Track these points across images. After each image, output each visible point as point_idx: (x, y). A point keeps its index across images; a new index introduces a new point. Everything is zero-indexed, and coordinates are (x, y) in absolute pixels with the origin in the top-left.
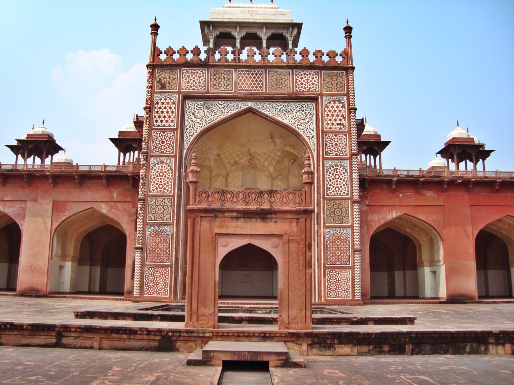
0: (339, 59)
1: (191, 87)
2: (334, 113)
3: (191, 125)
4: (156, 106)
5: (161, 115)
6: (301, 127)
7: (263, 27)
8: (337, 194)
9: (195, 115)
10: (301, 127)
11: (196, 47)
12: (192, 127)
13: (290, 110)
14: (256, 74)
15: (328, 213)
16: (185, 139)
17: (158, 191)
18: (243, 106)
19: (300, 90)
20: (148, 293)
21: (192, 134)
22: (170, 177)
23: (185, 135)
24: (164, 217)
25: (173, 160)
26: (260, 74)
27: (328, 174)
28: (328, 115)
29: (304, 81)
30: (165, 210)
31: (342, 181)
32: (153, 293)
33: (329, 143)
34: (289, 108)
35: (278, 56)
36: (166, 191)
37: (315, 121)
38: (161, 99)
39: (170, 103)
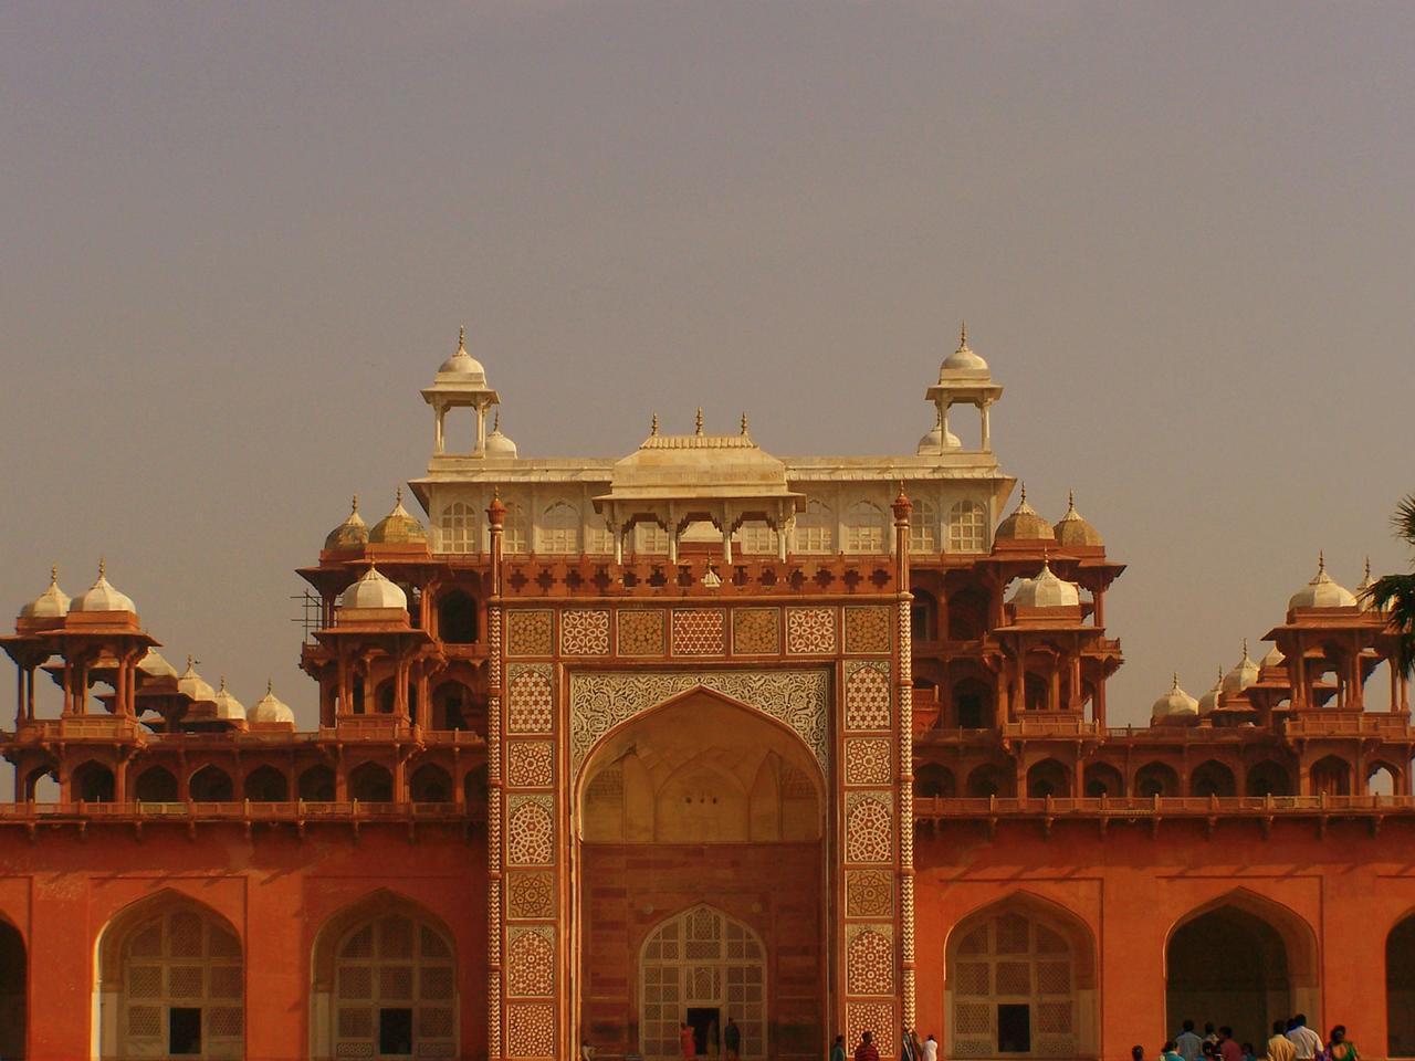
1: (581, 648)
5: (523, 708)
6: (799, 724)
10: (799, 724)
16: (572, 754)
18: (687, 684)
19: (797, 649)
20: (515, 1052)
21: (586, 743)
23: (572, 745)
25: (550, 797)
27: (852, 819)
28: (853, 700)
29: (805, 631)
31: (879, 832)
36: (540, 859)
38: (521, 676)
39: (541, 684)
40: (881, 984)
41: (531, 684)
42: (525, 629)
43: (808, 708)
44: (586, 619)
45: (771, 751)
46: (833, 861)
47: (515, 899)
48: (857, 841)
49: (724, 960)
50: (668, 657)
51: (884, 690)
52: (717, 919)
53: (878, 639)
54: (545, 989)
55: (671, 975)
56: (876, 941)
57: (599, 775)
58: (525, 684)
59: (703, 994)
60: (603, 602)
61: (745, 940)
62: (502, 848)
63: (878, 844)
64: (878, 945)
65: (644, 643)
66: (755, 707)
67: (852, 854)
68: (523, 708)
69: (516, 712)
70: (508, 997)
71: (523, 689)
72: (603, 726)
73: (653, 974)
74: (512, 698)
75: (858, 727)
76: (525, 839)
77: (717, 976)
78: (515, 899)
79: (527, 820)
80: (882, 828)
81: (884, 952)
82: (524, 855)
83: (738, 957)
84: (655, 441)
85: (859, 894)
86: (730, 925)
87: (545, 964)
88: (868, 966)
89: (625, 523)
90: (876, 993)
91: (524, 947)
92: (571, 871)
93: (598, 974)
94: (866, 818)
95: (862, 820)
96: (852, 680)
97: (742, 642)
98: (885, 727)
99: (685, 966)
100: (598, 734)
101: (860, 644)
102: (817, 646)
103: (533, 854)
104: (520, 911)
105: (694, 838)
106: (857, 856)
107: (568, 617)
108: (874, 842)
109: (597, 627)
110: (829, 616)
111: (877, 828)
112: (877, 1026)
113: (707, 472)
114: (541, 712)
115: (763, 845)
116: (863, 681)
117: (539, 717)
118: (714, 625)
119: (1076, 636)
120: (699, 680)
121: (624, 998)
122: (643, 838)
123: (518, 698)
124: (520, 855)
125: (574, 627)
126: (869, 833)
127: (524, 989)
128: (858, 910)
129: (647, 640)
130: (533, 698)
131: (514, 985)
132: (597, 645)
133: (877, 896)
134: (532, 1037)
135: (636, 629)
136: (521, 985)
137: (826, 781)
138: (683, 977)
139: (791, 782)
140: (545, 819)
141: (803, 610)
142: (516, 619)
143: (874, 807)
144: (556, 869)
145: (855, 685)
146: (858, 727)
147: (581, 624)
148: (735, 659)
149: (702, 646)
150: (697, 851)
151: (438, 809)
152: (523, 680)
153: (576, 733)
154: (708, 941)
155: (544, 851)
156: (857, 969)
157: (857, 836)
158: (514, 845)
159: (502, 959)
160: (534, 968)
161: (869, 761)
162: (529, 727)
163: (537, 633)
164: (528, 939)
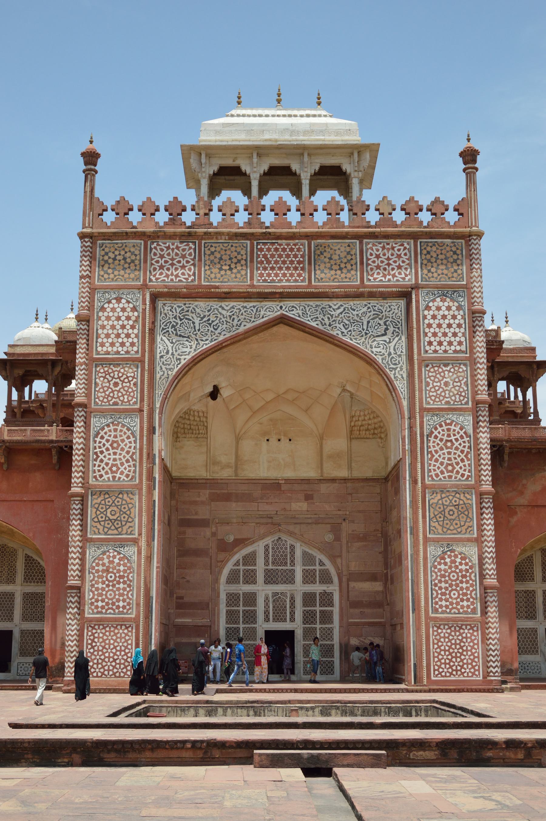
0: (451, 217)
2: (442, 321)
3: (170, 349)
4: (101, 314)
5: (110, 331)
6: (378, 350)
7: (302, 154)
8: (450, 477)
9: (175, 330)
10: (378, 350)
11: (176, 198)
12: (173, 354)
13: (355, 318)
14: (292, 250)
15: (432, 515)
16: (158, 376)
17: (109, 478)
19: (375, 279)
21: (171, 366)
22: (132, 450)
23: (158, 369)
24: (122, 526)
26: (299, 250)
27: (432, 439)
28: (430, 326)
29: (382, 262)
30: (125, 513)
31: (458, 452)
32: (103, 673)
33: (434, 381)
34: (355, 313)
35: (334, 213)
36: (123, 477)
37: (403, 338)
38: (109, 302)
39: (129, 310)
40: (465, 603)
41: (119, 310)
42: (114, 259)
43: (385, 334)
44: (173, 250)
45: (344, 390)
46: (414, 481)
47: (97, 516)
48: (437, 460)
49: (299, 587)
50: (253, 286)
51: (459, 317)
52: (292, 547)
53: (453, 271)
54: (124, 607)
55: (251, 599)
56: (458, 560)
57: (185, 413)
58: (113, 310)
59: (279, 617)
60: (190, 234)
61: (318, 567)
62: (86, 466)
63: (457, 464)
64: (461, 564)
65: (229, 272)
66: (334, 333)
67: (433, 473)
68: (110, 331)
69: (103, 336)
70: (86, 615)
71: (111, 314)
72: (188, 350)
73: (233, 599)
74: (100, 323)
75: (435, 351)
76: (108, 458)
77: (292, 599)
78: (97, 516)
79: (111, 439)
80: (461, 448)
81: (467, 571)
82: (107, 473)
84: (240, 112)
85: (440, 513)
86: (305, 554)
87: (124, 583)
88: (451, 585)
89: (212, 173)
90: (459, 613)
91: (104, 565)
92: (155, 489)
93: (182, 598)
94: (445, 438)
95: (441, 440)
96: (428, 308)
97: (322, 272)
98: (461, 351)
99: (263, 590)
100: (183, 357)
101: (435, 275)
102: (394, 276)
103: (116, 472)
104: (101, 528)
105: (273, 474)
106: (437, 475)
107: (155, 248)
108: (454, 461)
109: (184, 257)
110: (405, 248)
111: (457, 449)
112: (461, 647)
113: (287, 129)
114: (128, 336)
115: (333, 480)
116: (439, 309)
117: (125, 340)
118: (296, 256)
119: (535, 367)
120: (281, 307)
121: (205, 621)
122: (226, 474)
123: (106, 323)
124: (103, 472)
125: (162, 257)
126: (449, 453)
127: (103, 607)
128: (440, 528)
129: (231, 269)
130: (121, 323)
131: (92, 604)
132: (183, 274)
133: (459, 515)
134: (109, 657)
135: (221, 259)
136: (100, 604)
137: (405, 403)
139: (360, 423)
140: (128, 438)
141: (380, 243)
142: (107, 250)
143: (453, 427)
144: (139, 487)
145: (431, 313)
146: (435, 351)
147: (169, 254)
148: (316, 287)
149: (284, 275)
150: (273, 486)
151: (29, 433)
152: (111, 306)
153: (162, 357)
155: (126, 469)
156: (440, 588)
157: (436, 456)
158: (97, 463)
159: (82, 577)
160: (114, 586)
161: (446, 384)
162: (115, 349)
163: (126, 263)
164: (109, 557)
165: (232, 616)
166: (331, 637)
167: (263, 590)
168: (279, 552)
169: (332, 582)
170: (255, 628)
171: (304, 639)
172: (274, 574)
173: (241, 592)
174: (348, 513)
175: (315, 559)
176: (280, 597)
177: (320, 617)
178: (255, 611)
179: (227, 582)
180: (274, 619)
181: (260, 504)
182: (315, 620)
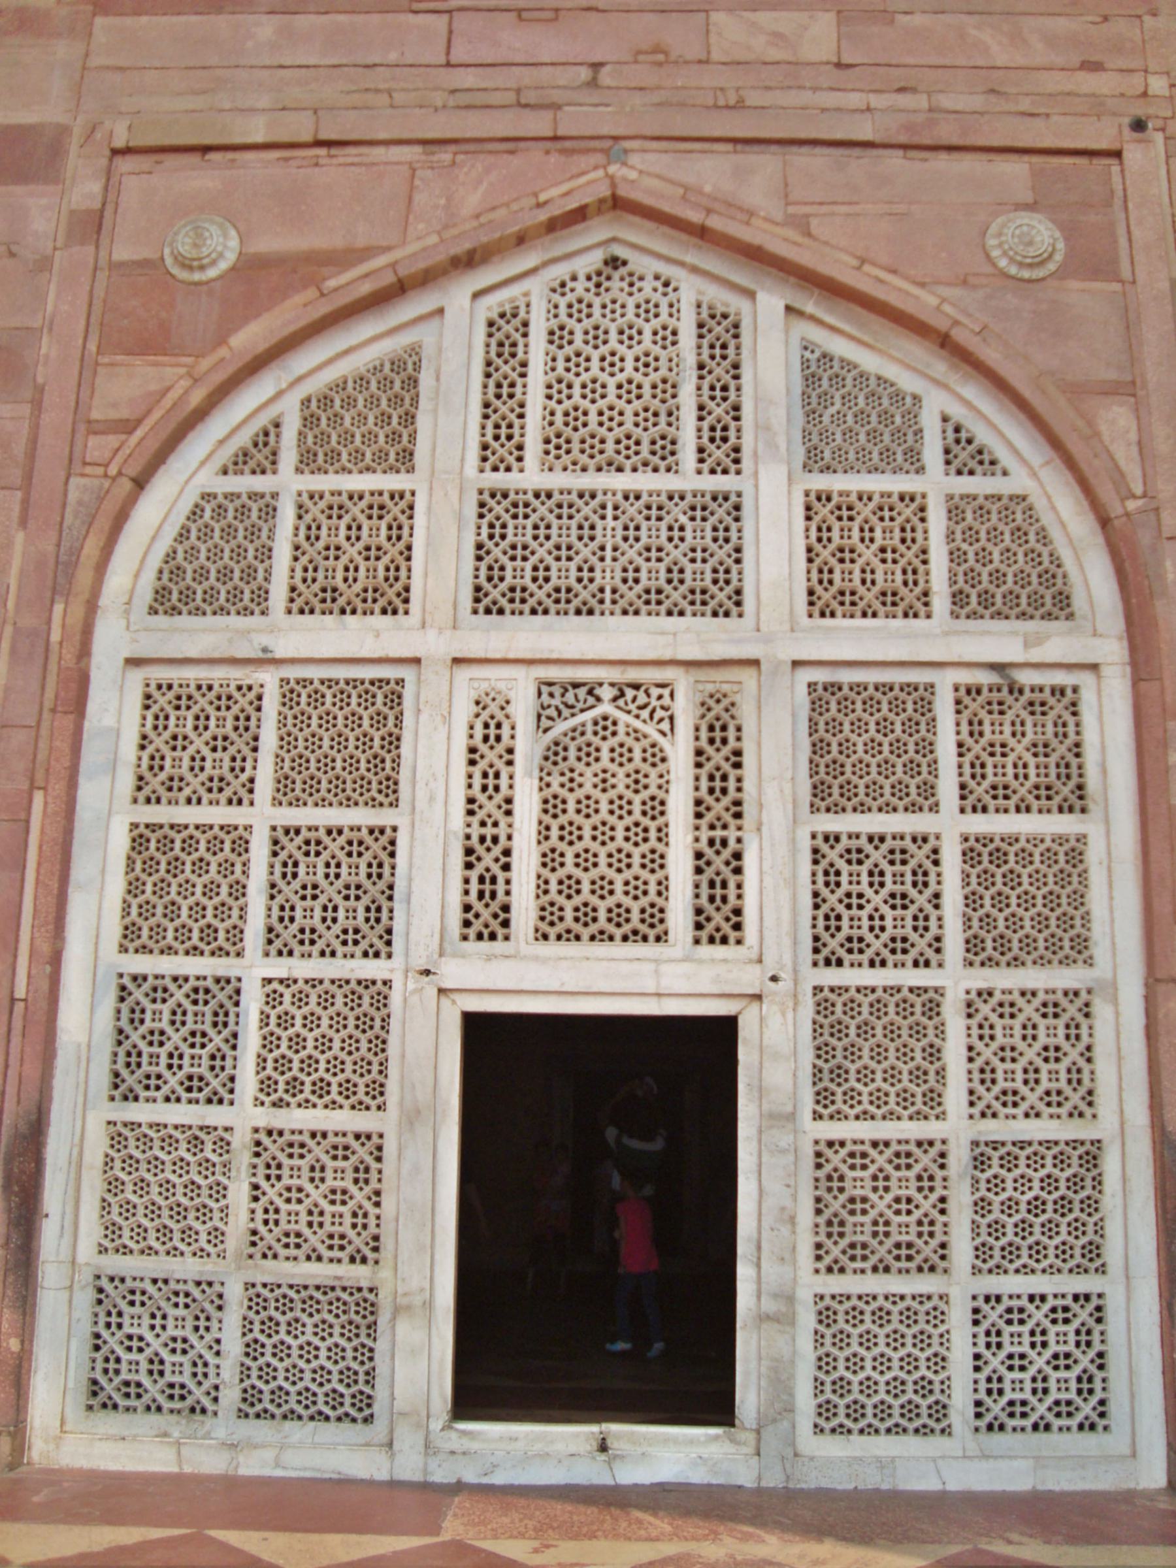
61: (935, 483)
73: (195, 732)
77: (719, 733)
83: (890, 598)
99: (456, 666)
138: (435, 757)
154: (644, 482)
165: (173, 879)
166: (1075, 1076)
167: (456, 666)
168: (611, 362)
169: (1063, 601)
170: (380, 992)
171: (823, 1097)
172: (564, 532)
173: (269, 680)
174: (1158, 85)
175: (912, 416)
176: (605, 725)
177: (972, 900)
178: (387, 838)
179: (161, 594)
180: (548, 915)
181: (461, 22)
182: (921, 923)
